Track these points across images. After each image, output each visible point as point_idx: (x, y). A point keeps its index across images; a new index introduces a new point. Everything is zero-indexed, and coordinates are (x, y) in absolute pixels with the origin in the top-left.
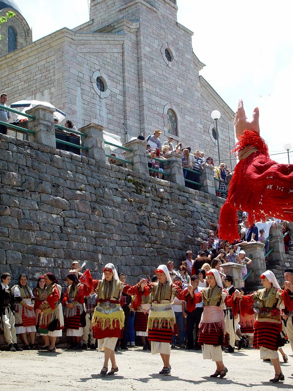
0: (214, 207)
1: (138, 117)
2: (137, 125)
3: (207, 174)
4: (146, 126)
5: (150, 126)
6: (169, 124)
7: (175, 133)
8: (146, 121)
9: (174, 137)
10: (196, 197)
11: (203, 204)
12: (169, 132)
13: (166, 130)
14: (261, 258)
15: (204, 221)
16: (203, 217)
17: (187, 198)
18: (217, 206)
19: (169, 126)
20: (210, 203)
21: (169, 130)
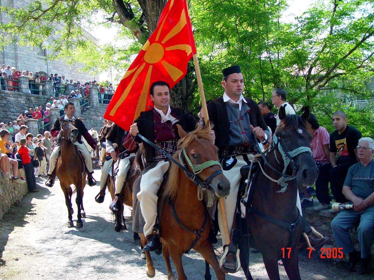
0: (26, 100)
1: (13, 47)
2: (12, 52)
3: (23, 82)
4: (18, 52)
5: (22, 52)
6: (38, 49)
7: (43, 54)
8: (18, 49)
9: (43, 57)
10: (11, 95)
11: (17, 99)
12: (38, 54)
13: (36, 53)
14: (34, 127)
15: (15, 109)
16: (14, 107)
17: (3, 96)
18: (29, 100)
19: (38, 51)
20: (23, 98)
21: (39, 53)
